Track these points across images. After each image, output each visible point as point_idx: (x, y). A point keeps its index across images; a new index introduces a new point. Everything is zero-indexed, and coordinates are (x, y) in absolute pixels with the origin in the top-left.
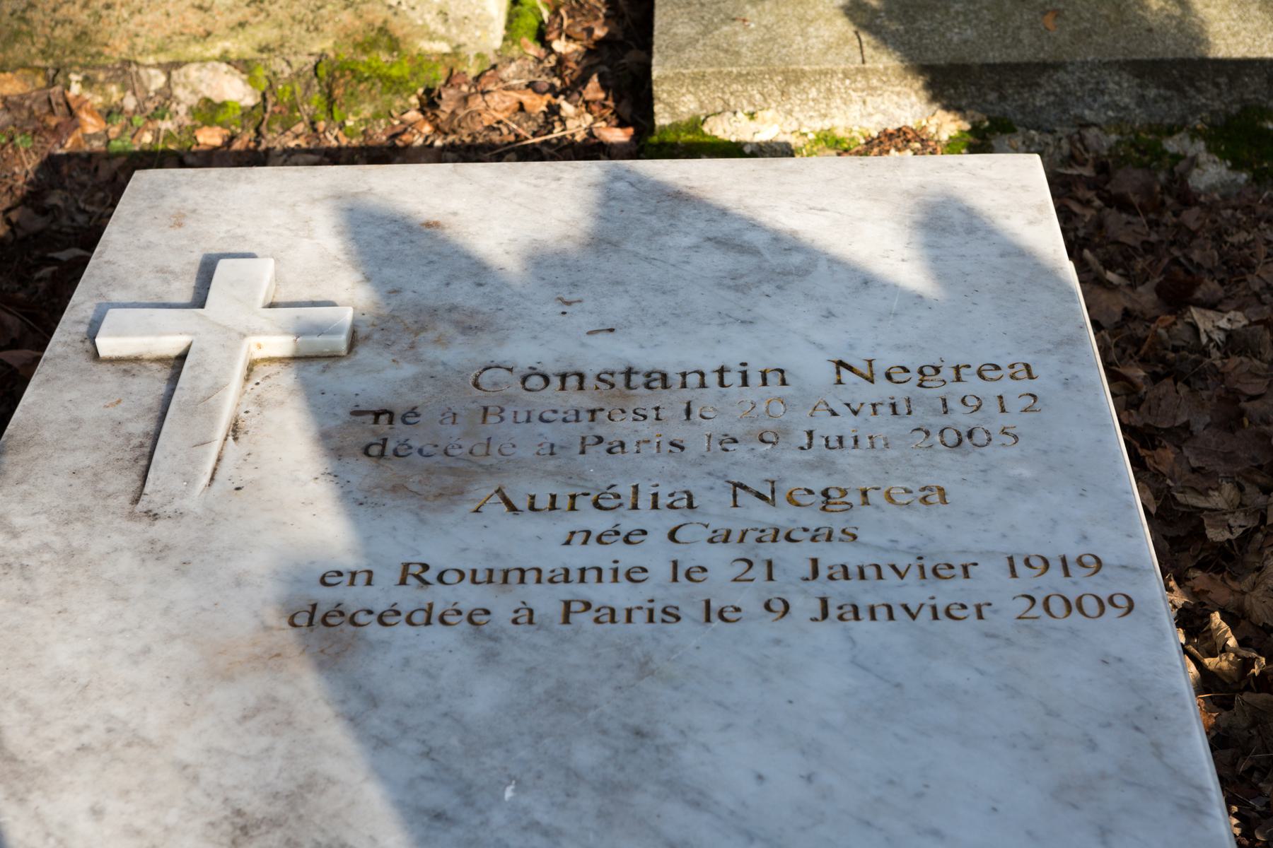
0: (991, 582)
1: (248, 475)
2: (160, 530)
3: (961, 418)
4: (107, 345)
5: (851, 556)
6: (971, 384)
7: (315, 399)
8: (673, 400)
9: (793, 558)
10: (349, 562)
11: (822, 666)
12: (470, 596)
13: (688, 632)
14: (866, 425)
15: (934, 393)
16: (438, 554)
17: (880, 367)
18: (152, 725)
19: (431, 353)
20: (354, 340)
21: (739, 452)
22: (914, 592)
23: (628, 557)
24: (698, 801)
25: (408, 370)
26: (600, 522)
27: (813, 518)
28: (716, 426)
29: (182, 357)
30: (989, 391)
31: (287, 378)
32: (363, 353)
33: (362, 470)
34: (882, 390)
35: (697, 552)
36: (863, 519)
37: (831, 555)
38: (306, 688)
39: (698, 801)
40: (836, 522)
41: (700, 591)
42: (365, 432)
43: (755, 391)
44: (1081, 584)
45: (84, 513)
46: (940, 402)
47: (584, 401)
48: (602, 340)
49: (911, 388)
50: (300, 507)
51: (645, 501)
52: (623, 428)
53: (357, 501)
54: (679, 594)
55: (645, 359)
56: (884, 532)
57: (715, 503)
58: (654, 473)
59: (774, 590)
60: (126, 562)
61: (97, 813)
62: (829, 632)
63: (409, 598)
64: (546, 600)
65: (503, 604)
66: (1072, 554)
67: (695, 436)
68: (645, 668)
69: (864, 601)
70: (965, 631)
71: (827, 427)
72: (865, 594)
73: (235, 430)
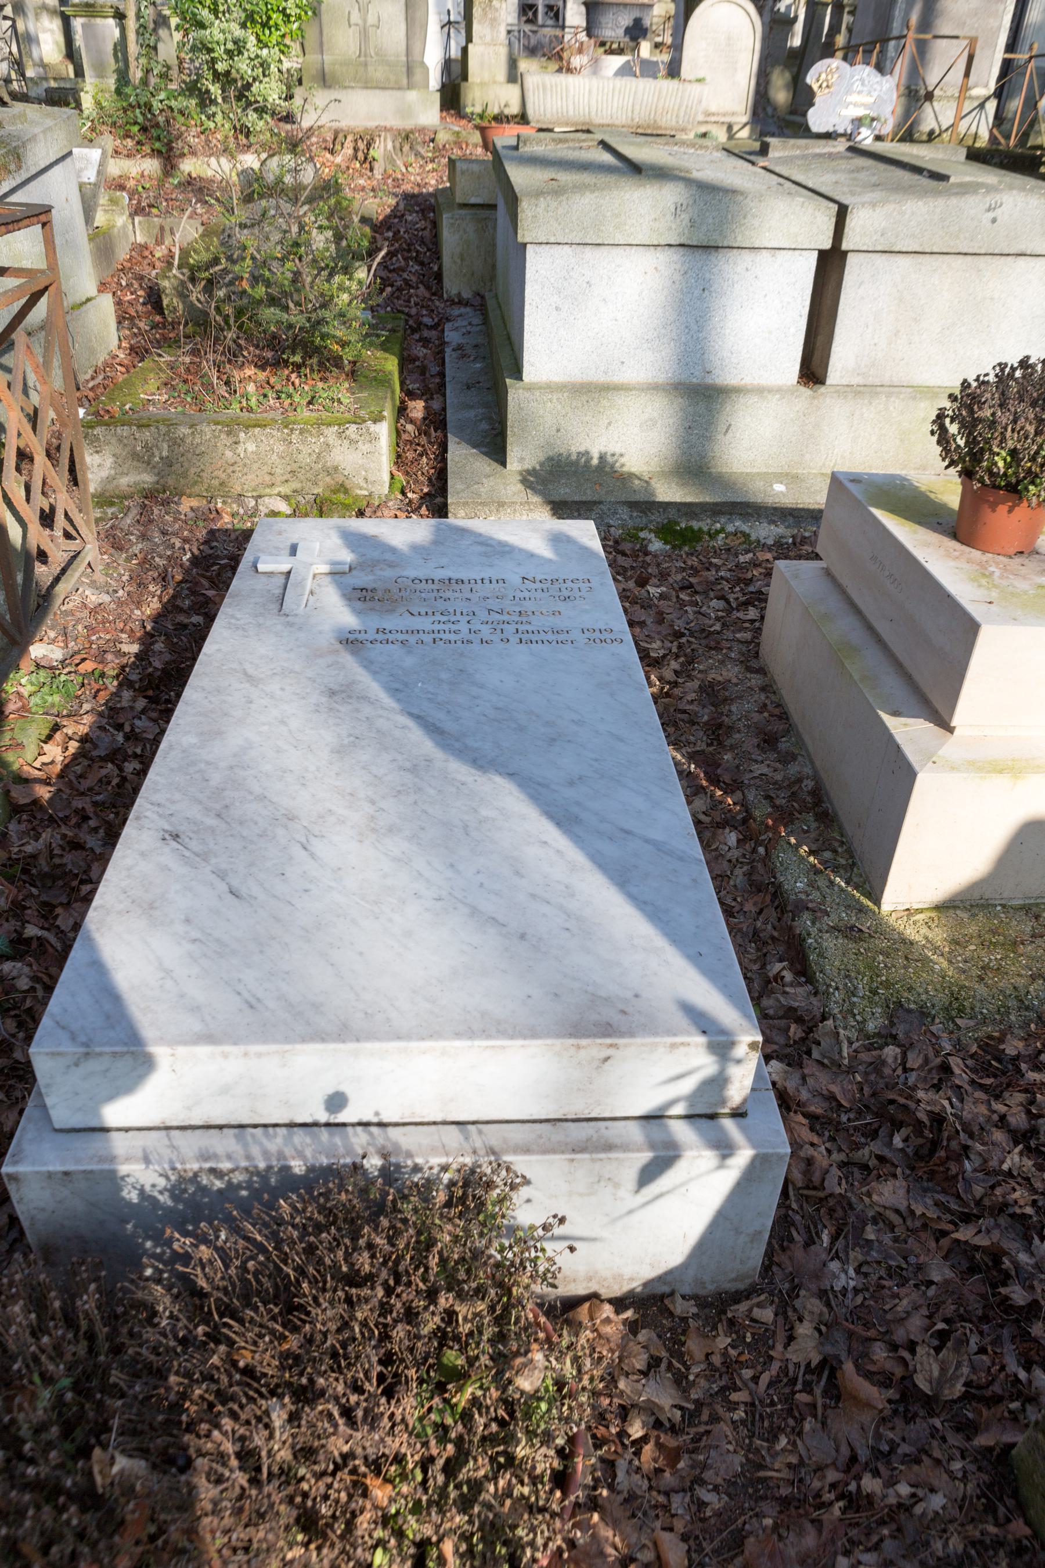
0: (576, 635)
1: (318, 605)
2: (290, 619)
3: (566, 593)
4: (261, 567)
5: (530, 628)
6: (569, 584)
7: (340, 586)
8: (466, 587)
9: (511, 628)
10: (358, 628)
11: (521, 655)
12: (401, 637)
13: (476, 646)
14: (533, 594)
15: (557, 586)
16: (388, 626)
17: (537, 579)
18: (297, 668)
19: (378, 573)
20: (350, 569)
21: (490, 601)
22: (550, 637)
23: (454, 627)
24: (482, 686)
25: (371, 577)
26: (443, 619)
27: (517, 618)
28: (481, 594)
29: (289, 572)
30: (575, 586)
31: (328, 579)
32: (354, 572)
33: (359, 604)
34: (538, 585)
35: (476, 625)
36: (532, 618)
37: (521, 628)
38: (348, 660)
39: (482, 686)
40: (524, 619)
41: (479, 636)
42: (358, 594)
43: (494, 585)
44: (605, 635)
45: (262, 615)
46: (559, 588)
47: (435, 587)
48: (440, 570)
49: (549, 585)
50: (338, 613)
51: (458, 613)
52: (448, 594)
53: (357, 612)
54: (472, 637)
55: (455, 576)
56: (537, 622)
57: (483, 615)
58: (461, 606)
59: (503, 636)
60: (279, 627)
61: (282, 689)
62: (522, 647)
63: (380, 637)
64: (428, 638)
65: (412, 639)
66: (603, 628)
67: (474, 597)
68: (462, 655)
69: (534, 640)
70: (568, 647)
71: (519, 595)
72: (534, 638)
73: (312, 593)
